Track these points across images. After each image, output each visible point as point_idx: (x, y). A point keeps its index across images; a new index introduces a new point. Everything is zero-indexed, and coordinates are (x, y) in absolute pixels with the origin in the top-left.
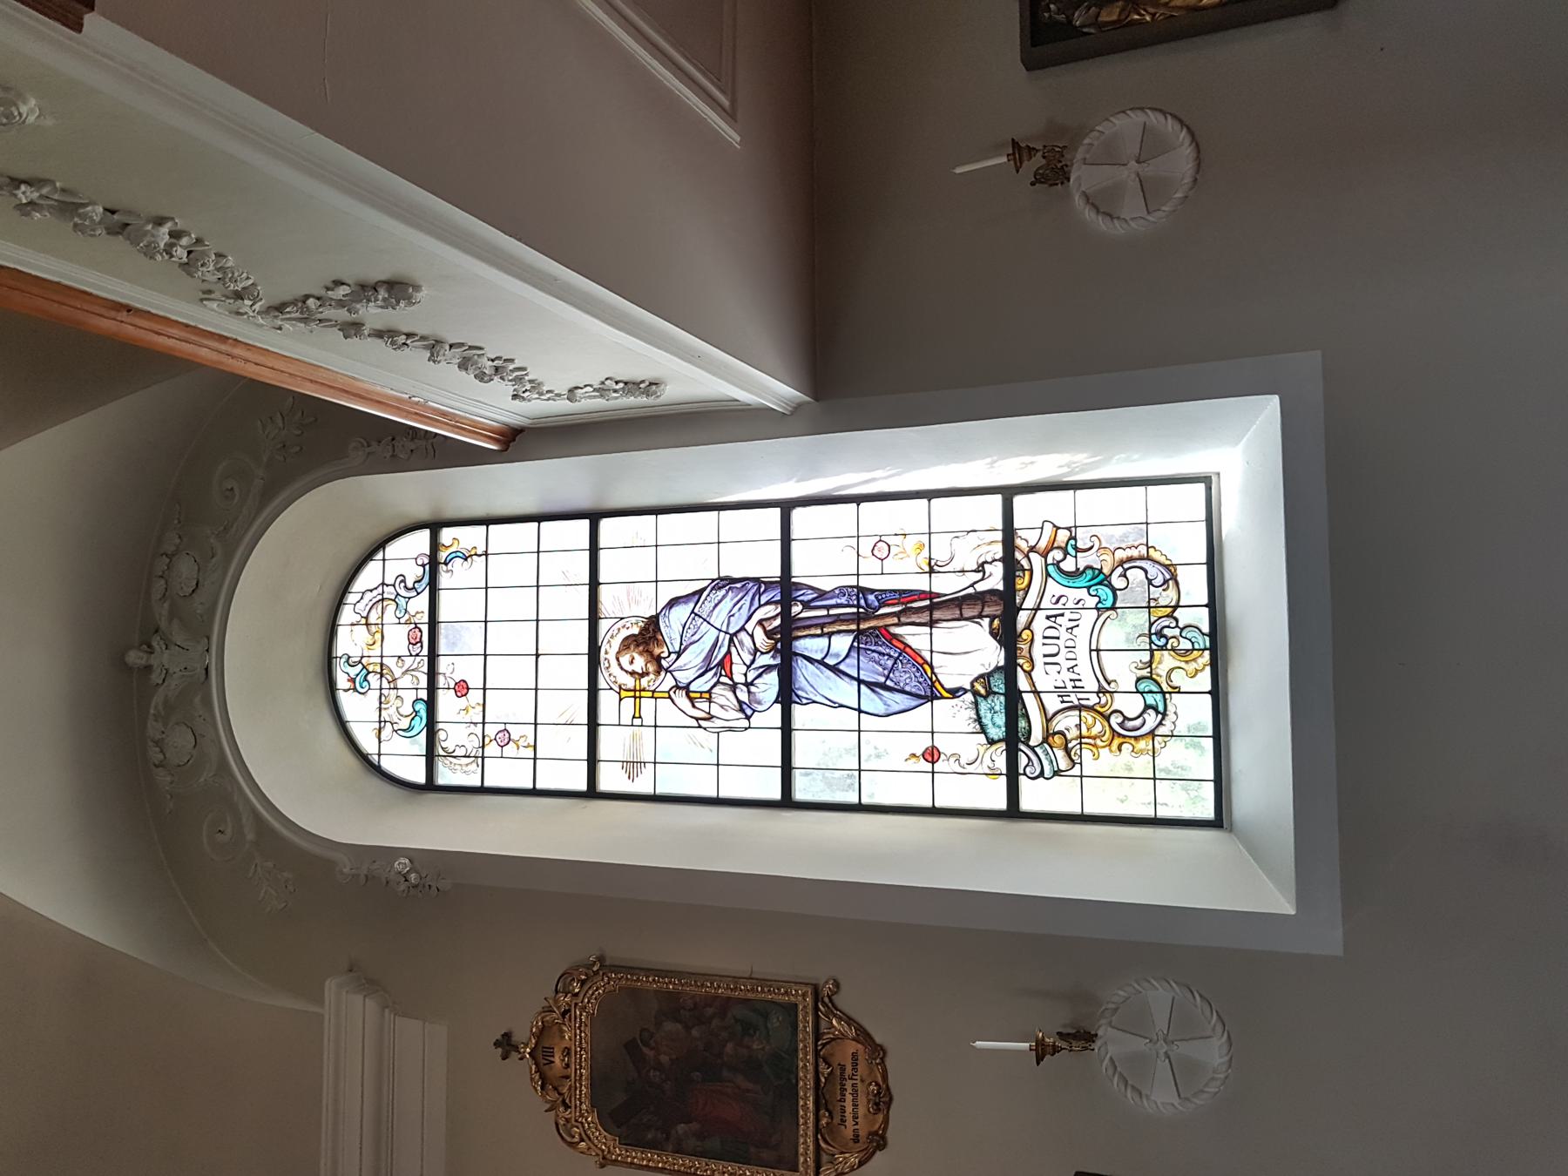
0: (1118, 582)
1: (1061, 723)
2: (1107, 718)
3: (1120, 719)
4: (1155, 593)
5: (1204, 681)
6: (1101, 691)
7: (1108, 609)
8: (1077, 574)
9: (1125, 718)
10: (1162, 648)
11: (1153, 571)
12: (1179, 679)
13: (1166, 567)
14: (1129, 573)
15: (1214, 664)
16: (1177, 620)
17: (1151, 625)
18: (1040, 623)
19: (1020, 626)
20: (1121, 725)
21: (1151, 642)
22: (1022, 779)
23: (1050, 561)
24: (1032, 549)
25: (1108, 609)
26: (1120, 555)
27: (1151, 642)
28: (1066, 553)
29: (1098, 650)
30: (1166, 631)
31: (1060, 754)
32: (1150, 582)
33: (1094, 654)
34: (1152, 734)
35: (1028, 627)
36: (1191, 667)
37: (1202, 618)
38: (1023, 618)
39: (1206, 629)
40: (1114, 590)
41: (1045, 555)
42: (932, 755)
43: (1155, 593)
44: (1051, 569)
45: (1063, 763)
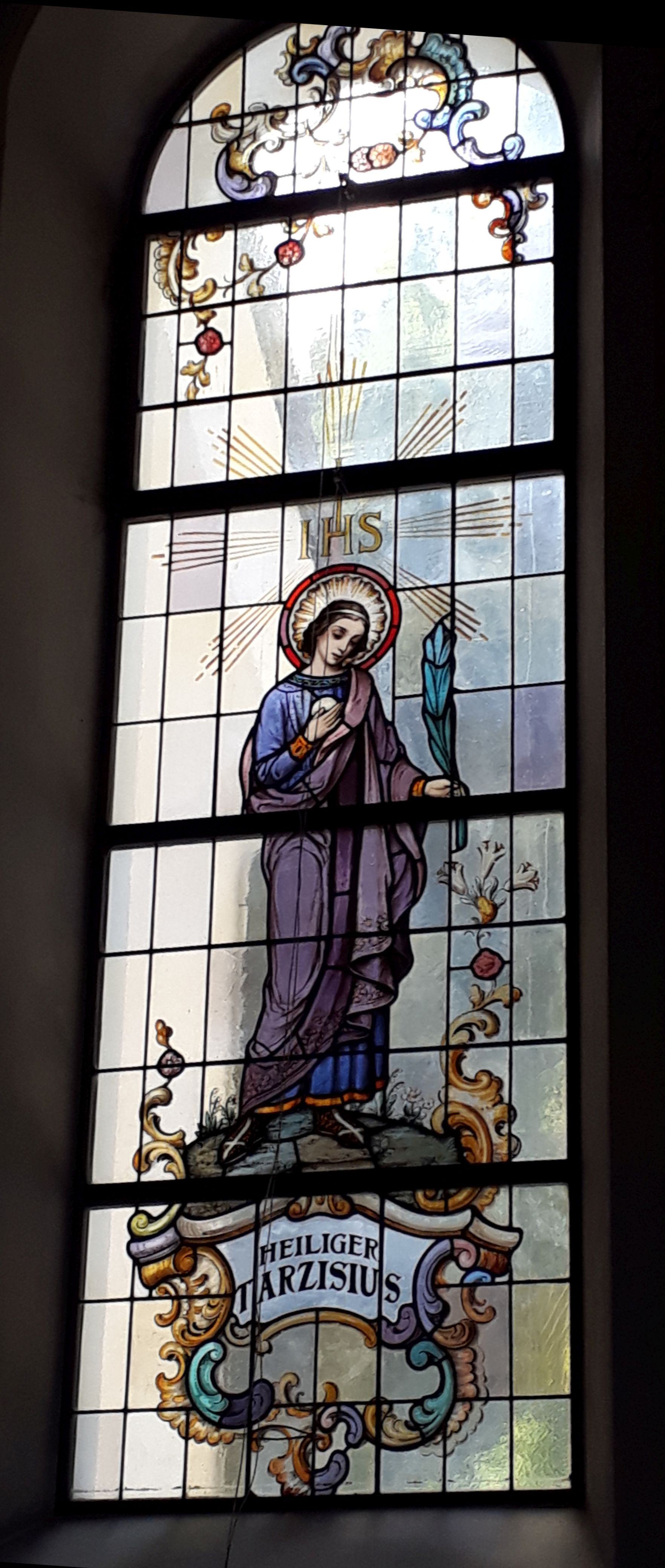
0: (420, 1349)
1: (207, 1265)
2: (214, 1339)
3: (213, 1355)
4: (402, 1412)
5: (266, 1488)
6: (256, 1326)
7: (379, 1334)
8: (435, 1286)
9: (217, 1363)
10: (316, 1424)
11: (439, 1405)
12: (273, 1448)
13: (443, 1426)
14: (434, 1369)
15: (287, 1503)
16: (356, 1446)
17: (352, 1405)
18: (361, 1227)
19: (358, 1199)
20: (207, 1357)
21: (326, 1405)
22: (131, 1211)
23: (460, 1243)
24: (477, 1214)
25: (379, 1334)
26: (463, 1356)
27: (326, 1405)
28: (468, 1271)
29: (317, 1322)
30: (342, 1427)
31: (166, 1264)
32: (418, 1403)
33: (311, 1315)
34: (192, 1408)
35: (356, 1210)
36: (288, 1466)
37: (359, 1484)
38: (371, 1201)
39: (341, 1491)
40: (407, 1346)
41: (464, 1233)
42: (172, 1065)
43: (402, 1412)
44: (445, 1245)
45: (151, 1270)
